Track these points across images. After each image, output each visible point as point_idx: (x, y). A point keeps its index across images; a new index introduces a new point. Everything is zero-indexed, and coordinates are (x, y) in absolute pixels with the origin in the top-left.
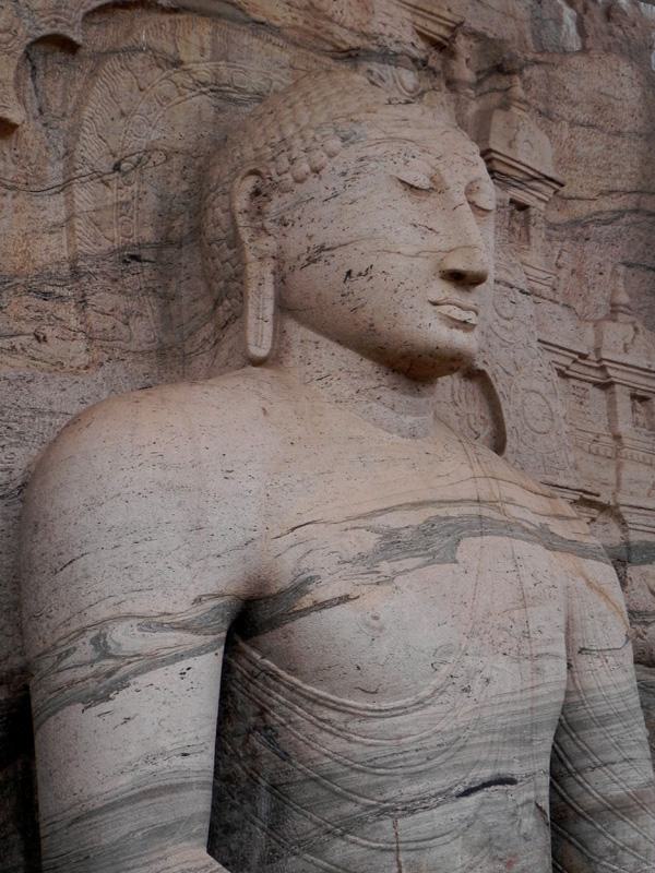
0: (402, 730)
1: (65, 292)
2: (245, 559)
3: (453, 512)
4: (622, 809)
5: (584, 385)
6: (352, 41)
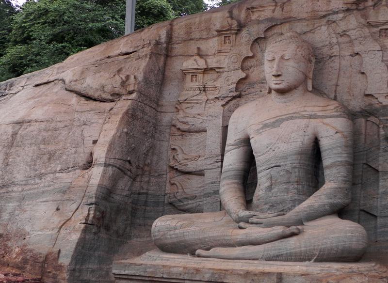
3: (284, 117)
4: (328, 167)
6: (324, 13)
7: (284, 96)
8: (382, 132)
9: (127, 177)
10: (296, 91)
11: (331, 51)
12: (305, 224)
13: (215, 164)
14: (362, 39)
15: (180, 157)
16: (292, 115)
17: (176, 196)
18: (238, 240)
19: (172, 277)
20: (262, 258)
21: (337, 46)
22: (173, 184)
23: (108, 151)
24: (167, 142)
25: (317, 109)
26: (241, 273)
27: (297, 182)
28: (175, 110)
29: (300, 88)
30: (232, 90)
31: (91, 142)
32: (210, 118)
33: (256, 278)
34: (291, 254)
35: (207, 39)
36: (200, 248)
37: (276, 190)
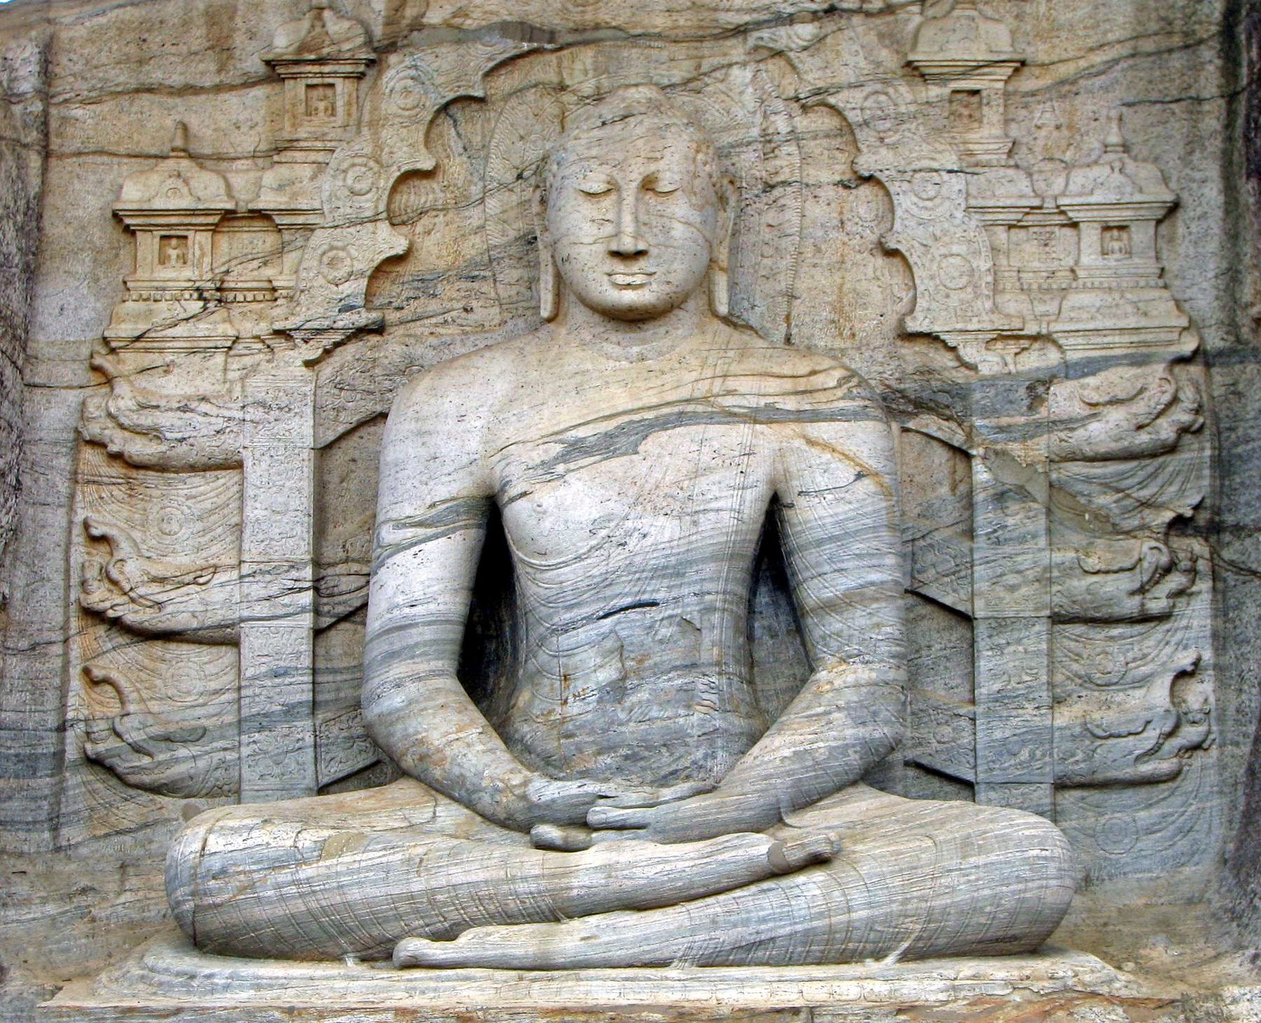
0: (563, 578)
1: (488, 274)
2: (471, 474)
3: (650, 415)
4: (830, 607)
5: (1048, 229)
7: (640, 335)
8: (981, 474)
10: (681, 313)
12: (788, 821)
13: (287, 600)
14: (888, 125)
15: (132, 570)
17: (119, 728)
18: (575, 892)
21: (792, 148)
22: (95, 683)
25: (772, 385)
27: (718, 664)
28: (85, 376)
30: (351, 301)
32: (254, 413)
34: (808, 937)
36: (410, 933)
37: (643, 695)
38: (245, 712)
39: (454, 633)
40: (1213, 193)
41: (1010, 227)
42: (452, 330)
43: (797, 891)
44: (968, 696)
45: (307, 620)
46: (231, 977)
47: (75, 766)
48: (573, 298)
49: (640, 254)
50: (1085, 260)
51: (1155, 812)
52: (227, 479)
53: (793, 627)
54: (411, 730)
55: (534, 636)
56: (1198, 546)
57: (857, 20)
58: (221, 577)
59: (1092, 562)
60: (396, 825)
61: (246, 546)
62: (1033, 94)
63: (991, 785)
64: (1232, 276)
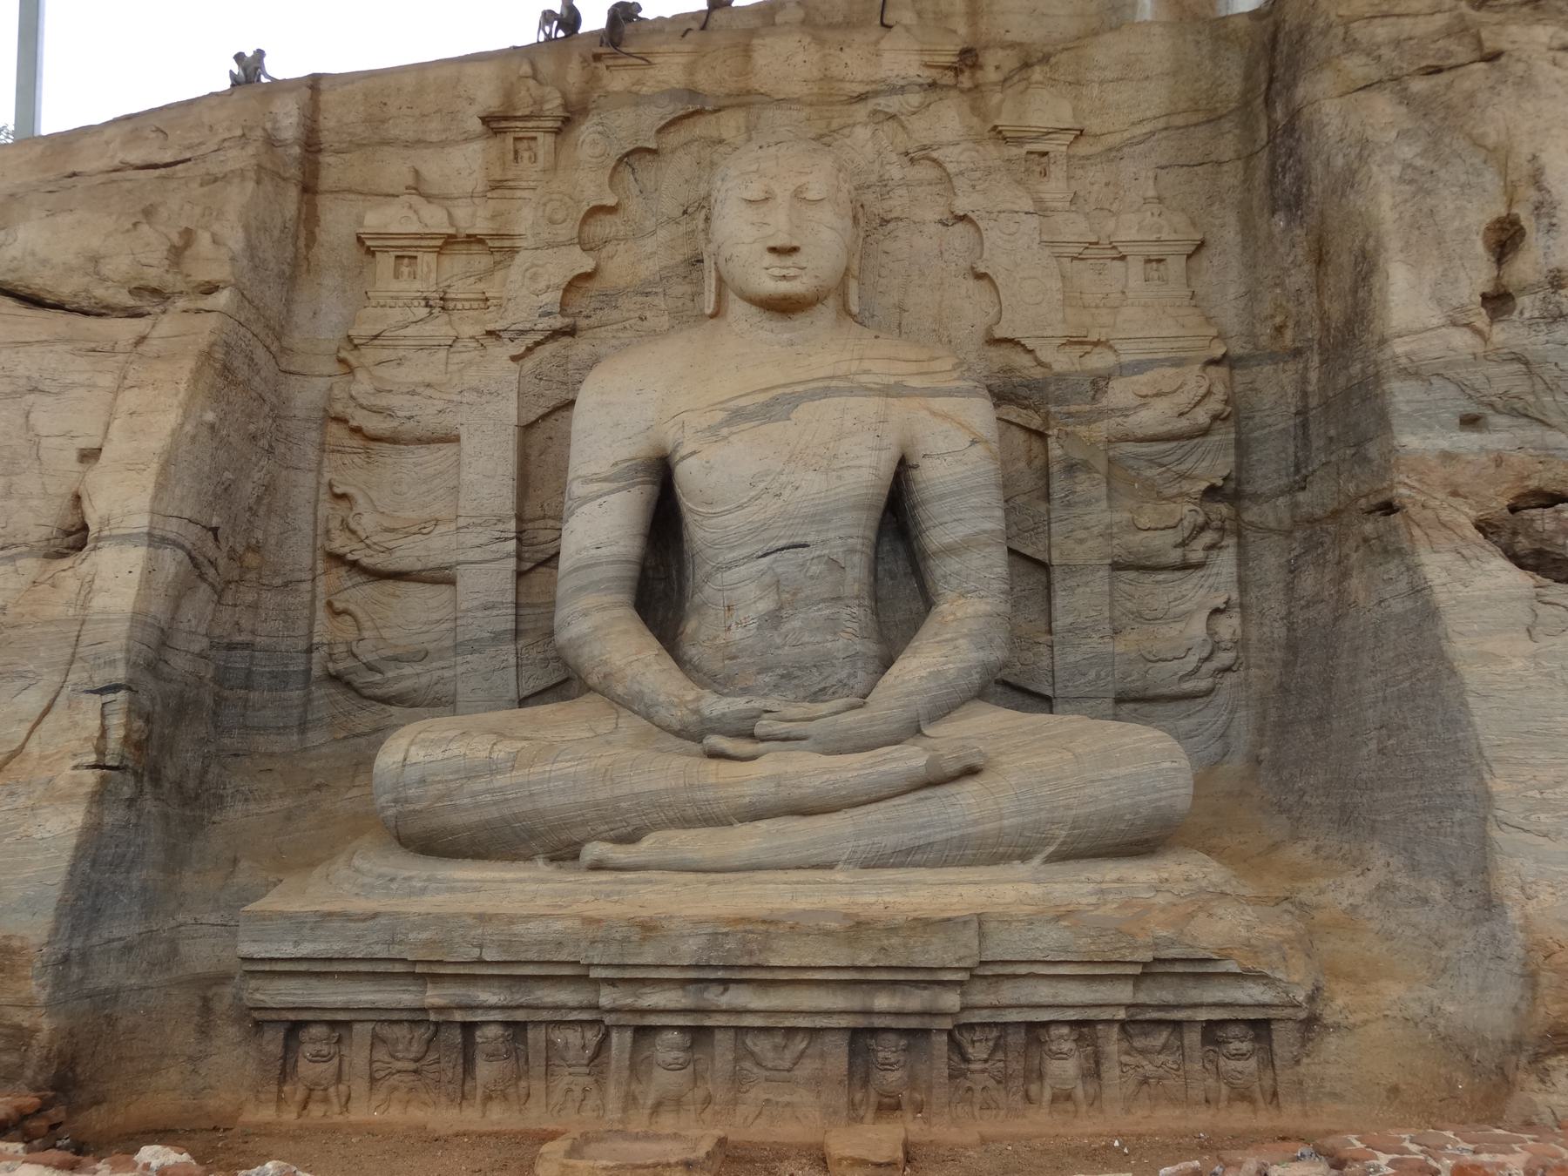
3: (800, 388)
4: (950, 550)
6: (861, 89)
7: (790, 324)
8: (1055, 451)
9: (204, 586)
11: (887, 204)
12: (926, 732)
13: (494, 547)
14: (978, 174)
15: (367, 523)
16: (826, 383)
19: (522, 957)
20: (848, 862)
22: (337, 613)
23: (161, 487)
24: (311, 476)
26: (833, 925)
27: (857, 597)
28: (332, 367)
29: (831, 302)
30: (548, 309)
31: (74, 455)
32: (470, 397)
33: (895, 941)
34: (962, 843)
35: (443, 144)
37: (797, 623)
38: (460, 638)
39: (632, 571)
40: (1230, 235)
41: (1073, 258)
42: (629, 334)
43: (953, 800)
44: (1044, 627)
45: (511, 564)
46: (428, 880)
47: (320, 680)
48: (732, 296)
49: (795, 250)
50: (1132, 284)
51: (1194, 720)
52: (449, 449)
53: (909, 570)
54: (596, 653)
55: (700, 575)
56: (1224, 509)
57: (953, 93)
58: (442, 529)
59: (1144, 521)
60: (584, 735)
61: (461, 504)
62: (1087, 158)
63: (1067, 700)
64: (1251, 295)
